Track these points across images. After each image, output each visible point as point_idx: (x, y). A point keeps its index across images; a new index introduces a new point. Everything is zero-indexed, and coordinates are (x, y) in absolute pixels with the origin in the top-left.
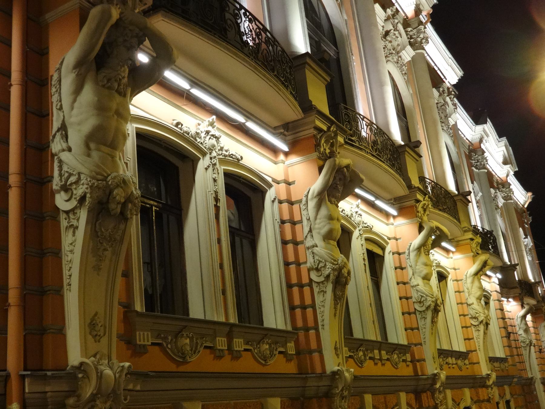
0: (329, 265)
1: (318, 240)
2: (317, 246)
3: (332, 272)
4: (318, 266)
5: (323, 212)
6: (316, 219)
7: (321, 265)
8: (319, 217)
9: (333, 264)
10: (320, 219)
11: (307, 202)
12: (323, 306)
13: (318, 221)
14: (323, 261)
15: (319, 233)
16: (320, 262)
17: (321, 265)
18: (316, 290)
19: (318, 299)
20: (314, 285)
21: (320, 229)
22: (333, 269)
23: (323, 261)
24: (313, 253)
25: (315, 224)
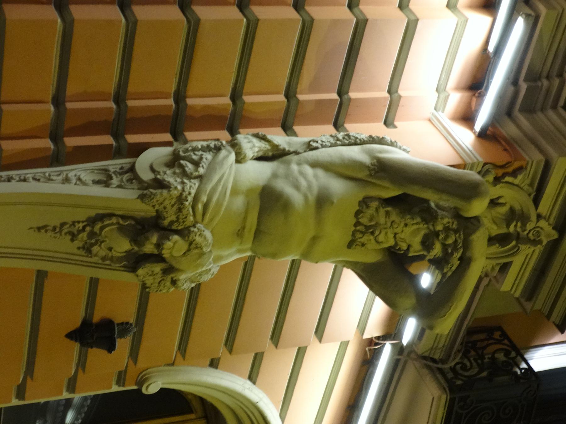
0: (192, 186)
1: (256, 173)
2: (238, 161)
3: (175, 193)
4: (184, 158)
5: (337, 186)
6: (315, 165)
7: (189, 167)
8: (320, 172)
9: (196, 199)
10: (316, 176)
11: (356, 144)
12: (67, 180)
13: (309, 170)
14: (201, 171)
15: (275, 176)
16: (197, 164)
17: (189, 167)
18: (113, 164)
19: (84, 171)
20: (125, 162)
21: (288, 176)
22: (181, 199)
23: (201, 171)
24: (218, 149)
25: (299, 164)
